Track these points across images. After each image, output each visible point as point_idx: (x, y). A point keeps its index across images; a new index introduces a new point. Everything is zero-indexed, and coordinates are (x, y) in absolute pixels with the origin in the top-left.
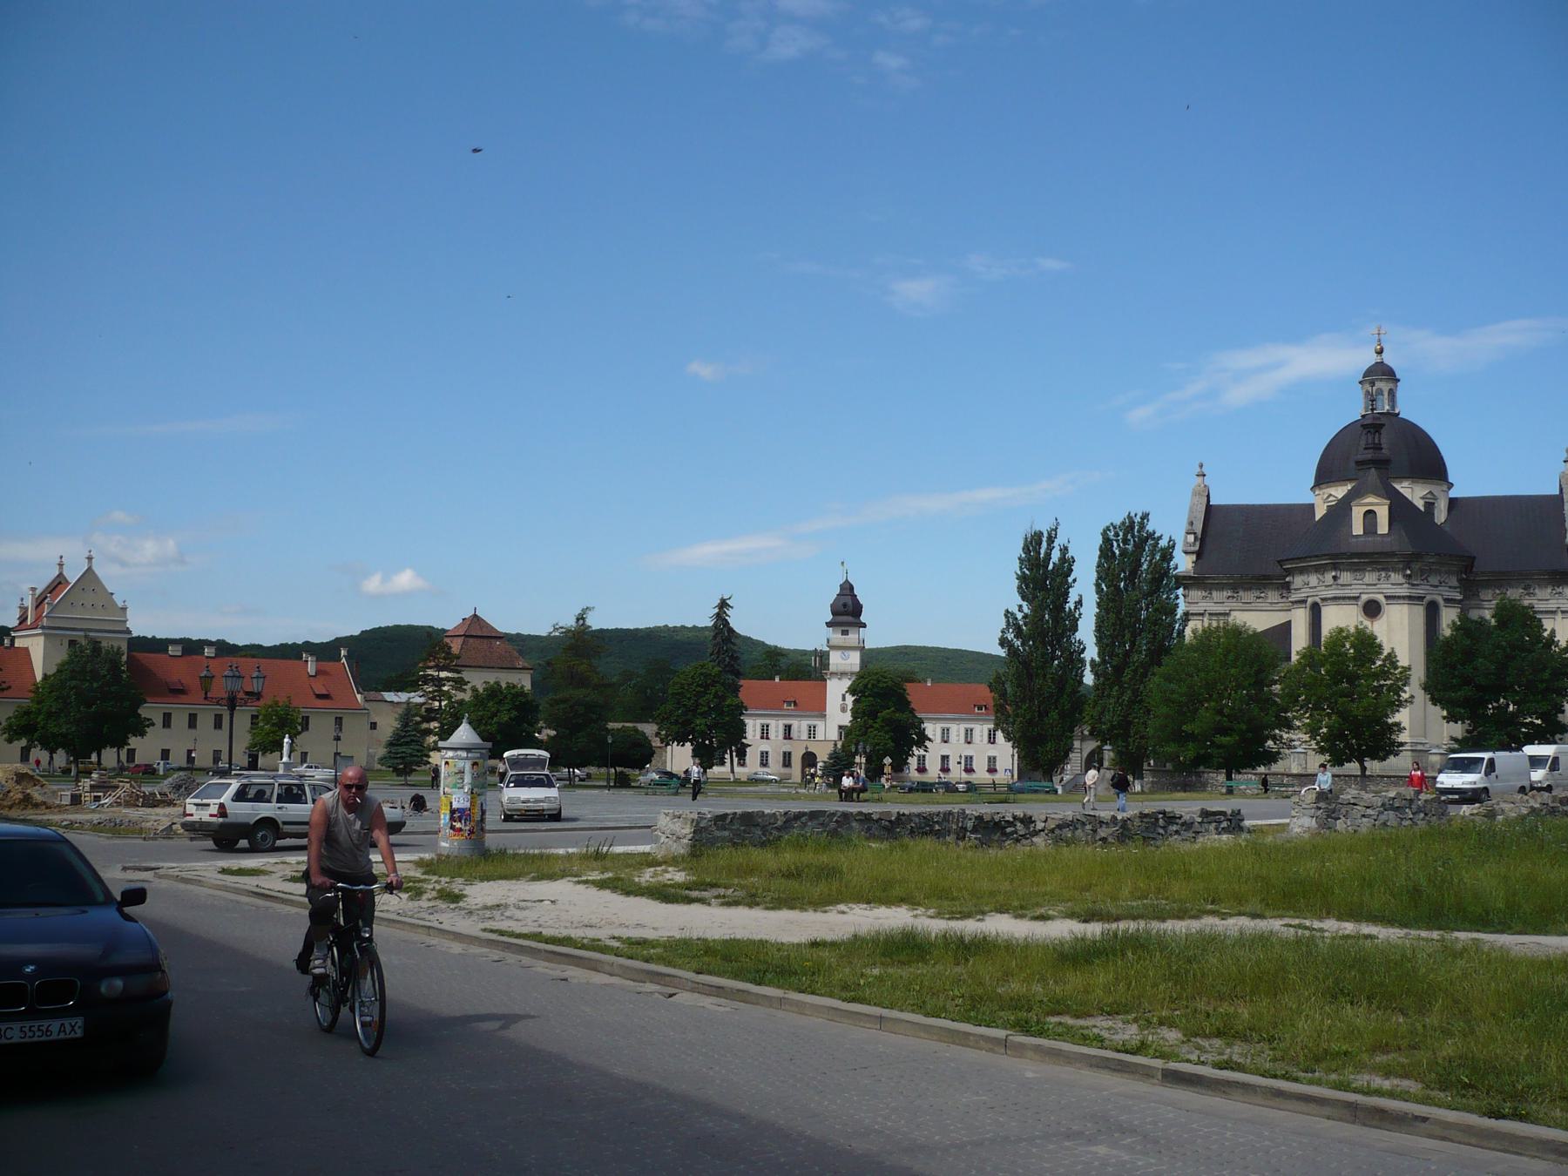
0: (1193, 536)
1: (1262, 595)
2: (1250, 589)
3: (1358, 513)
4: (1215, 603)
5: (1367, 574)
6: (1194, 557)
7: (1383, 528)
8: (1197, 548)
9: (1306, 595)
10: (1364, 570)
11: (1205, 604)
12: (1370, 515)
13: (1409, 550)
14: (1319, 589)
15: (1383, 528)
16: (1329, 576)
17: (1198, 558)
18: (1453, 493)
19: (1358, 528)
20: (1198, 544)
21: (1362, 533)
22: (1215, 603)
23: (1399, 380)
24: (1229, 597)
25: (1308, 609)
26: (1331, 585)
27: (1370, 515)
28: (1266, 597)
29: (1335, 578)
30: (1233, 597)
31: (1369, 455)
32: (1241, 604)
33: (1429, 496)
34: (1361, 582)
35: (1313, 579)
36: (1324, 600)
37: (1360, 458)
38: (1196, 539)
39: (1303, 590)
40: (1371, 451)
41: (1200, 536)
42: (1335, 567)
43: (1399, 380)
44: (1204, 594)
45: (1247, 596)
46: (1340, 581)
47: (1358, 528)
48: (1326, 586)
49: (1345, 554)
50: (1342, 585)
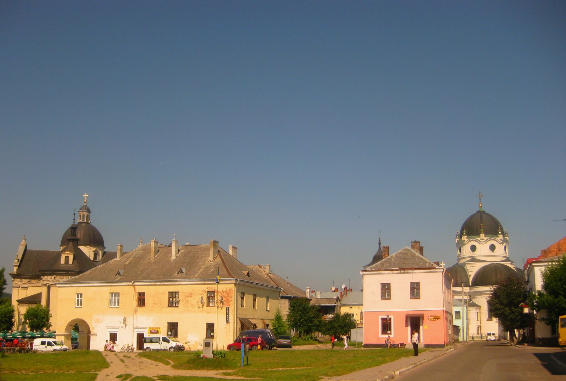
0: (17, 260)
1: (39, 281)
2: (35, 279)
3: (63, 256)
4: (23, 283)
5: (65, 276)
6: (17, 267)
7: (71, 262)
8: (18, 264)
9: (46, 283)
10: (64, 275)
11: (20, 284)
12: (67, 257)
13: (78, 270)
14: (50, 281)
15: (71, 262)
16: (53, 277)
17: (18, 268)
18: (105, 250)
19: (63, 261)
20: (19, 263)
21: (64, 263)
22: (23, 283)
23: (91, 212)
24: (28, 281)
25: (47, 287)
26: (53, 280)
27: (67, 257)
28: (40, 282)
29: (55, 278)
30: (29, 282)
31: (71, 237)
32: (32, 284)
33: (96, 251)
34: (63, 279)
35: (49, 278)
36: (51, 285)
37: (68, 238)
38: (18, 261)
39: (46, 281)
40: (72, 236)
41: (20, 260)
42: (55, 274)
43: (91, 212)
44: (20, 280)
45: (34, 281)
46: (56, 279)
47: (63, 261)
48: (52, 280)
49: (57, 270)
50: (57, 280)
